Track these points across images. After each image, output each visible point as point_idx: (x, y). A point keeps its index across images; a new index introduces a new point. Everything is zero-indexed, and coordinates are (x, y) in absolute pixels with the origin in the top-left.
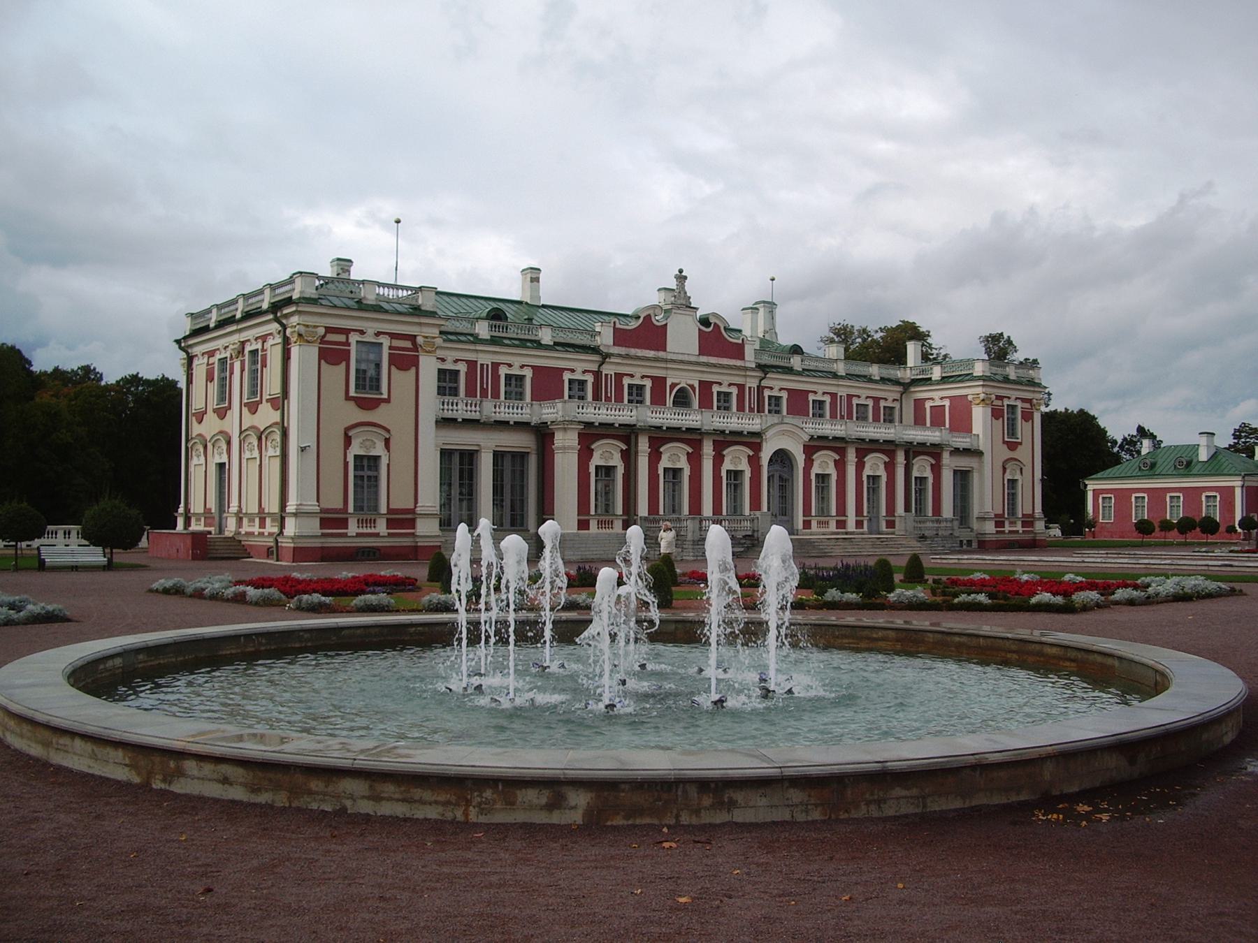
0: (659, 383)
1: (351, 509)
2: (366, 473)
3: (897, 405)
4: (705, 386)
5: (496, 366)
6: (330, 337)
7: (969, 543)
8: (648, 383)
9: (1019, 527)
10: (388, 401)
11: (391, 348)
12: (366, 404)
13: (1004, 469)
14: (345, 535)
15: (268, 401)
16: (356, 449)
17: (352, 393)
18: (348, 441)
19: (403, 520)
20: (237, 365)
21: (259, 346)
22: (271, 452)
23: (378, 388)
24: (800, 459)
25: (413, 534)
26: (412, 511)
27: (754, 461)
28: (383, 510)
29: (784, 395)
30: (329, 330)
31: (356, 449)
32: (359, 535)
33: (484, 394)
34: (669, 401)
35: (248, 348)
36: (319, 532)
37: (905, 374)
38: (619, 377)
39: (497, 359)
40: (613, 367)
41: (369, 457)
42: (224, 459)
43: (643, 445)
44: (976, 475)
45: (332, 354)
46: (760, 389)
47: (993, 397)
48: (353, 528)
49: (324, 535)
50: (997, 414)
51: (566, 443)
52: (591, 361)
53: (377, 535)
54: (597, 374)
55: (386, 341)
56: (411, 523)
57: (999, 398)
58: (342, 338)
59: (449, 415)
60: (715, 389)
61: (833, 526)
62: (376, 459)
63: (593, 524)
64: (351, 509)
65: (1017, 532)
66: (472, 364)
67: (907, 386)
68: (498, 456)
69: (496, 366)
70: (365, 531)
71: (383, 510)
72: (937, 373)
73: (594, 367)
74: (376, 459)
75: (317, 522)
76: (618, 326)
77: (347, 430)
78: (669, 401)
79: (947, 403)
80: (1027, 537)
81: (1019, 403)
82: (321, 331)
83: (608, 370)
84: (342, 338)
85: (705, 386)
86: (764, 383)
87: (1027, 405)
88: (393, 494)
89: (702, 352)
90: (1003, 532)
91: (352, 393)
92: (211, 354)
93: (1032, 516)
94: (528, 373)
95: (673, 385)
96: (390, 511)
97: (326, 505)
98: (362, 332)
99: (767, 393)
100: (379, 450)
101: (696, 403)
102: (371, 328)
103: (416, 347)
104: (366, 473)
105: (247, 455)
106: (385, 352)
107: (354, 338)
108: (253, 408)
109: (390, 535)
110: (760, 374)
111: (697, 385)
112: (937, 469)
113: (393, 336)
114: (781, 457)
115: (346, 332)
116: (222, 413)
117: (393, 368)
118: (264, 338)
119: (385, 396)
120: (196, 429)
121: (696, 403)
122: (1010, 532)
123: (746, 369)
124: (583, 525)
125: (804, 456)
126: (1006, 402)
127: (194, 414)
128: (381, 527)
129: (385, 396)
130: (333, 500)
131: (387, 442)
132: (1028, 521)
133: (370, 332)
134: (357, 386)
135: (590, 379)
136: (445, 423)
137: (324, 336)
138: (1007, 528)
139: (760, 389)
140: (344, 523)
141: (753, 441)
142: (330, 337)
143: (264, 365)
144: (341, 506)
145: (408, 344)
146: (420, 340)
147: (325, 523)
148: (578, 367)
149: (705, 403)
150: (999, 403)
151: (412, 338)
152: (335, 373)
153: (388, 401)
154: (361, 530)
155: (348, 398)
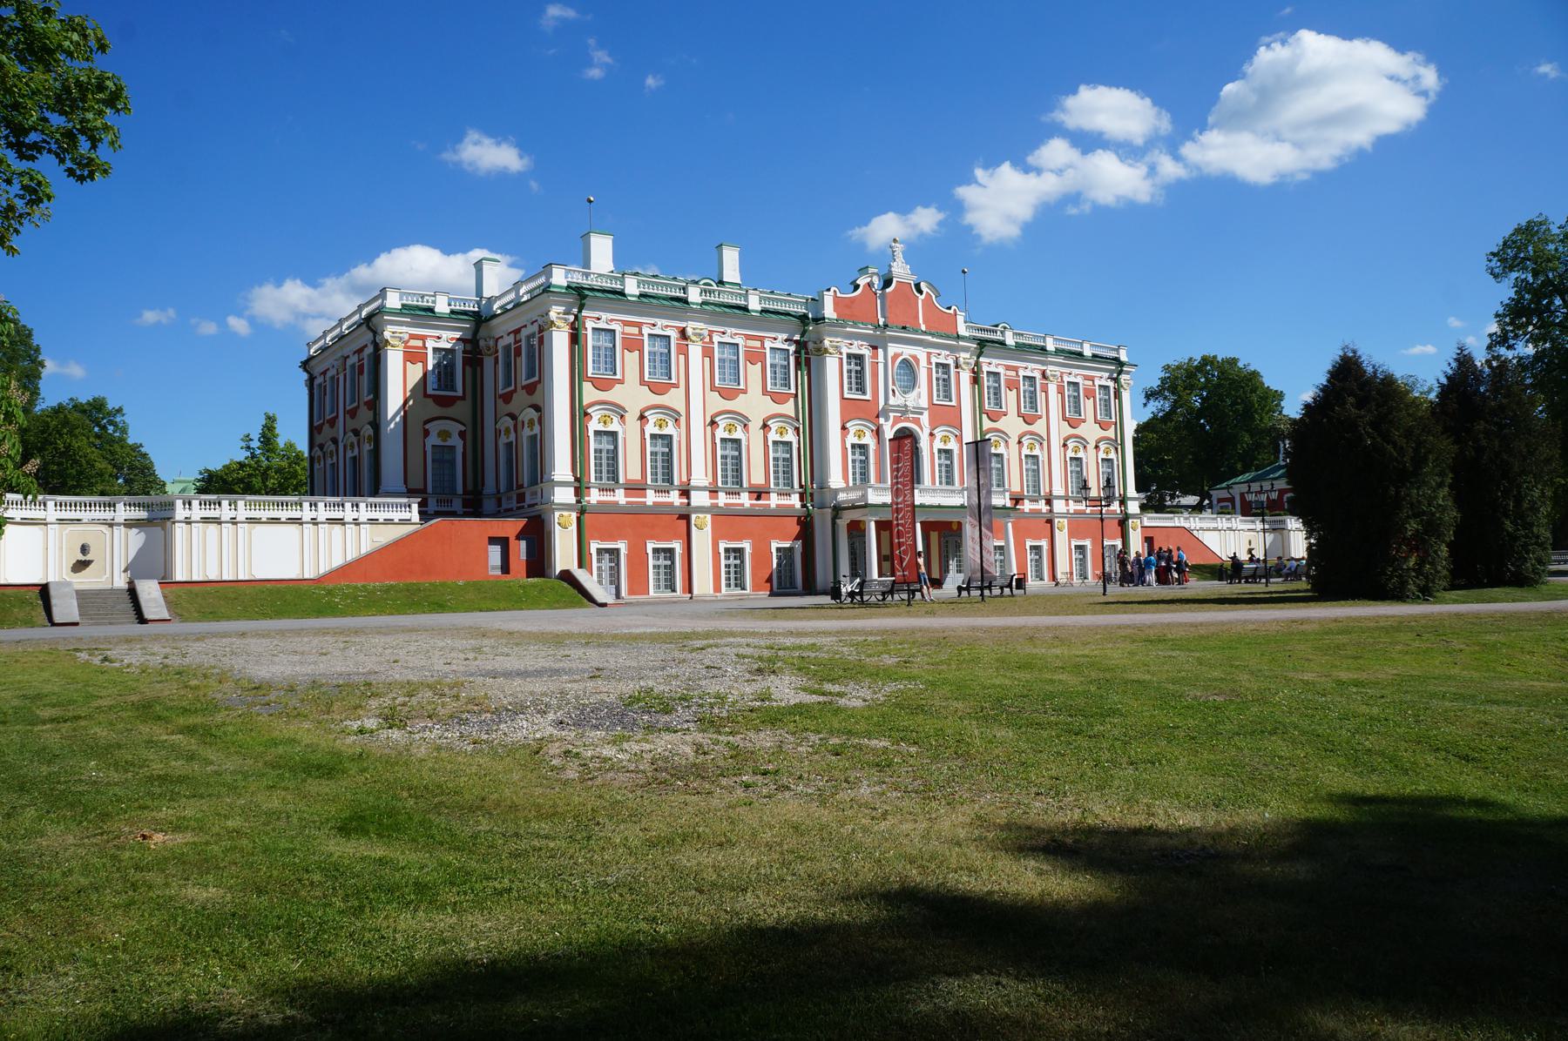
1: (430, 489)
6: (413, 343)
16: (434, 440)
17: (430, 391)
18: (426, 433)
23: (453, 389)
28: (460, 490)
30: (413, 337)
31: (434, 440)
62: (452, 448)
77: (426, 422)
91: (430, 391)
96: (465, 492)
119: (460, 393)
129: (460, 393)
142: (413, 343)
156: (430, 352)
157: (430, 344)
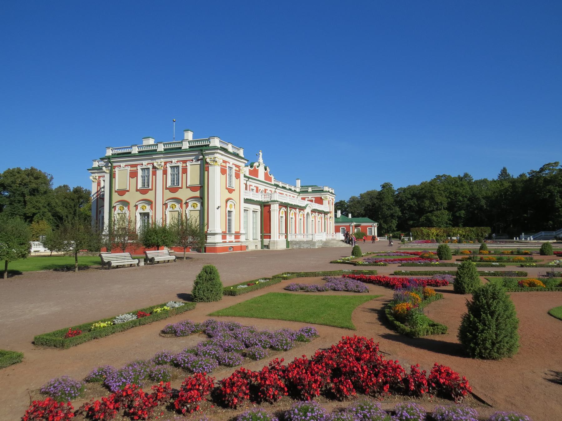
0: (257, 188)
4: (266, 190)
12: (231, 191)
14: (225, 242)
15: (187, 187)
16: (228, 209)
20: (159, 173)
21: (180, 165)
22: (190, 208)
30: (224, 162)
32: (230, 242)
35: (168, 165)
36: (222, 241)
37: (298, 190)
38: (250, 185)
42: (148, 209)
51: (275, 208)
53: (232, 242)
55: (234, 168)
58: (224, 164)
67: (299, 193)
71: (233, 231)
72: (310, 190)
79: (314, 199)
82: (221, 161)
83: (248, 183)
84: (224, 164)
85: (266, 190)
92: (136, 166)
102: (232, 161)
103: (239, 171)
105: (168, 209)
107: (228, 165)
108: (173, 190)
109: (236, 242)
113: (236, 166)
114: (308, 214)
116: (143, 192)
118: (184, 162)
120: (116, 197)
123: (272, 185)
127: (116, 192)
128: (232, 238)
133: (231, 163)
143: (185, 171)
145: (237, 169)
146: (241, 168)
155: (227, 188)
156: (227, 169)
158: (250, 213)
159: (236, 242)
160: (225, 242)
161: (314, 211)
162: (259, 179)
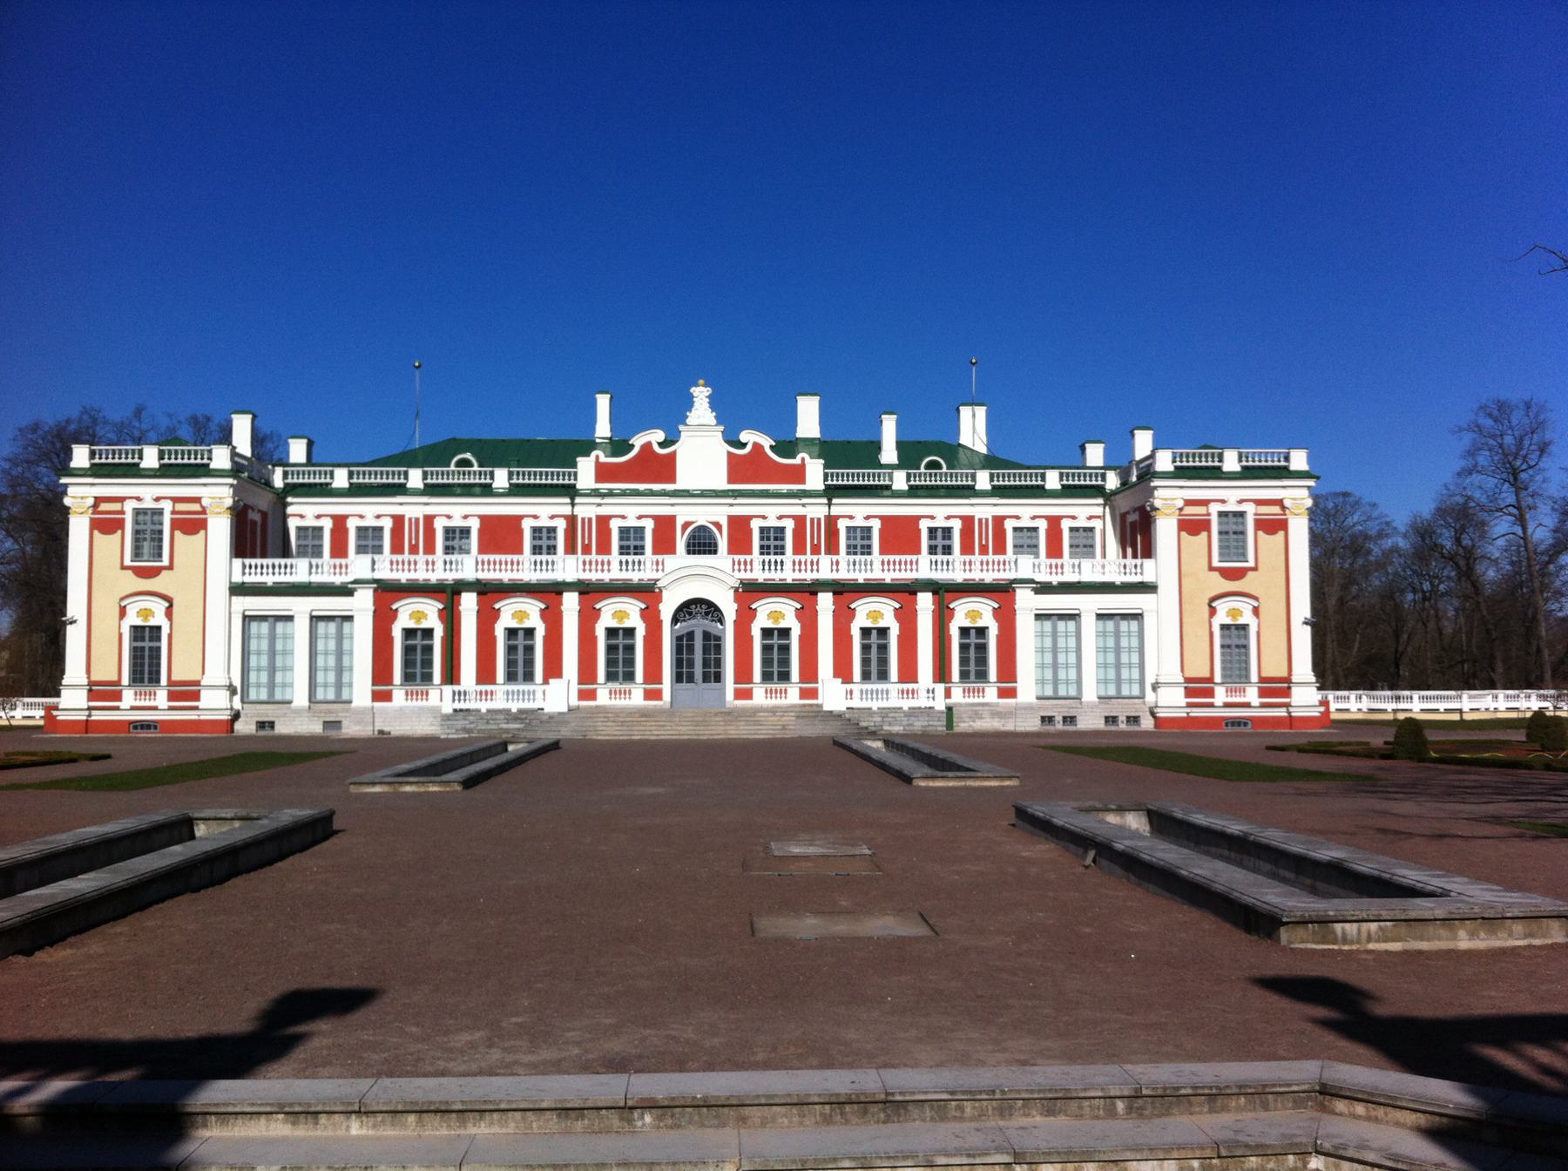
2: (147, 644)
3: (1097, 524)
5: (429, 520)
7: (1133, 720)
8: (649, 525)
9: (1252, 695)
10: (170, 567)
11: (173, 512)
13: (1213, 611)
14: (117, 708)
16: (133, 619)
19: (186, 692)
24: (729, 610)
25: (196, 708)
26: (197, 683)
27: (651, 616)
29: (876, 525)
30: (98, 500)
33: (414, 550)
34: (681, 544)
36: (84, 704)
38: (603, 521)
39: (430, 510)
40: (594, 508)
41: (151, 628)
43: (469, 601)
44: (1149, 621)
45: (105, 525)
46: (831, 521)
47: (1180, 503)
48: (129, 698)
49: (90, 709)
50: (1191, 526)
52: (561, 506)
53: (155, 708)
54: (571, 520)
55: (167, 506)
56: (196, 696)
57: (1189, 503)
58: (116, 506)
59: (238, 578)
60: (755, 525)
61: (793, 695)
62: (159, 628)
63: (399, 695)
64: (125, 681)
65: (1247, 705)
66: (398, 520)
68: (315, 619)
69: (429, 520)
70: (142, 703)
71: (164, 681)
73: (567, 510)
74: (159, 628)
75: (84, 693)
76: (603, 459)
77: (122, 599)
78: (681, 544)
80: (1282, 713)
81: (1250, 509)
82: (91, 501)
86: (835, 511)
87: (1276, 509)
88: (179, 664)
89: (730, 481)
90: (1211, 705)
91: (127, 562)
93: (1288, 680)
94: (474, 524)
95: (686, 525)
97: (94, 678)
98: (138, 499)
99: (842, 525)
100: (159, 619)
101: (723, 543)
103: (204, 512)
104: (147, 644)
106: (167, 519)
107: (129, 506)
109: (171, 708)
110: (825, 501)
111: (724, 523)
112: (1006, 617)
113: (176, 500)
115: (121, 500)
117: (177, 533)
119: (166, 562)
121: (723, 543)
122: (1227, 705)
124: (381, 696)
125: (735, 606)
126: (1214, 509)
130: (104, 672)
131: (169, 613)
132: (1276, 688)
134: (137, 554)
135: (561, 525)
136: (238, 590)
137: (95, 506)
138: (1220, 696)
139: (831, 521)
140: (117, 696)
141: (647, 593)
142: (104, 507)
144: (115, 678)
145: (195, 507)
147: (93, 695)
148: (544, 512)
149: (740, 543)
150: (1201, 510)
151: (197, 500)
152: (108, 544)
153: (170, 567)
154: (138, 703)
155: (123, 568)
157: (129, 506)
158: (301, 627)
159: (171, 708)
160: (117, 708)
161: (750, 592)
162: (680, 484)
